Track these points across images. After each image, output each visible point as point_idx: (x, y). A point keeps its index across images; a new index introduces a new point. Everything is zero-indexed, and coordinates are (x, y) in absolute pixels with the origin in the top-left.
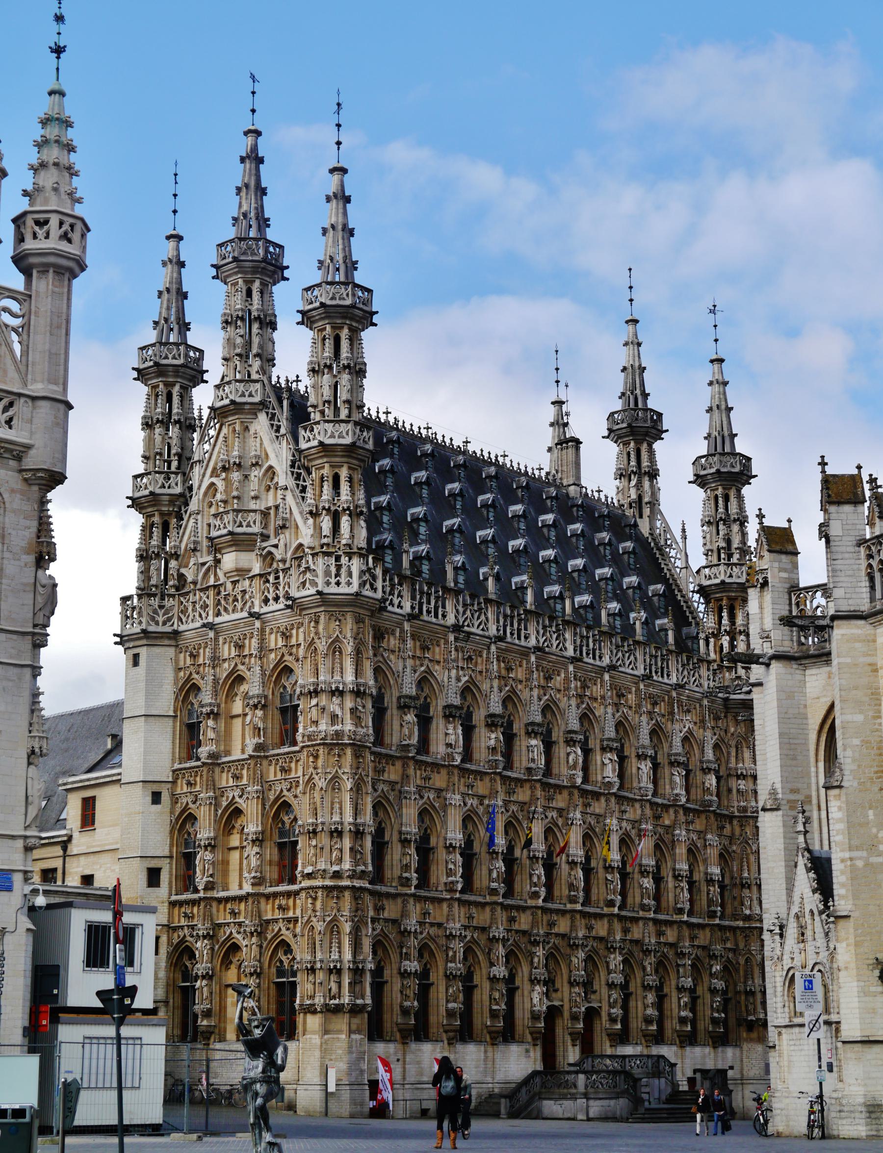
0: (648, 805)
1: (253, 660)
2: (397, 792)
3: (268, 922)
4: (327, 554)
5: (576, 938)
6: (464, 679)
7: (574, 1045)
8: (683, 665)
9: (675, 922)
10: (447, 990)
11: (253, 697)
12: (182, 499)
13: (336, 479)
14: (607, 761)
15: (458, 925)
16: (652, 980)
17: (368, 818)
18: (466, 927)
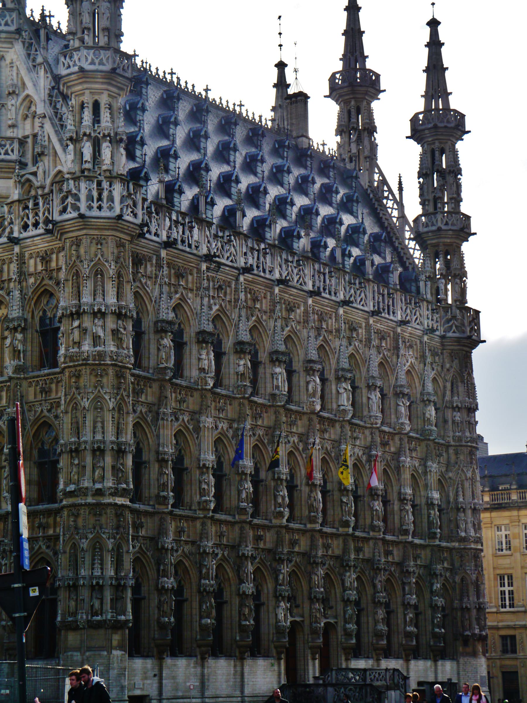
0: (377, 433)
1: (12, 285)
4: (89, 179)
5: (316, 556)
6: (215, 308)
7: (314, 659)
9: (401, 542)
11: (13, 320)
13: (96, 106)
14: (342, 391)
15: (210, 544)
16: (382, 596)
17: (129, 437)
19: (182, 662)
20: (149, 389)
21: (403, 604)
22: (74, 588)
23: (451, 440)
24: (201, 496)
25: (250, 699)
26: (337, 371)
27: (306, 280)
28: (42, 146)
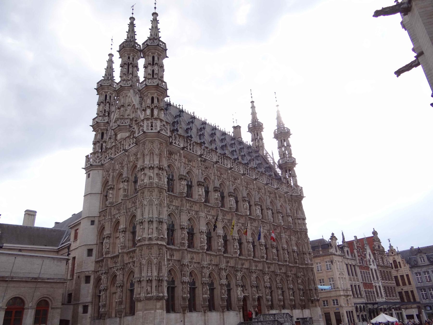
3: (127, 264)
5: (252, 269)
10: (203, 289)
15: (206, 263)
17: (164, 216)
18: (209, 264)
19: (194, 315)
20: (176, 201)
22: (140, 281)
23: (298, 229)
24: (201, 244)
26: (255, 202)
28: (136, 118)
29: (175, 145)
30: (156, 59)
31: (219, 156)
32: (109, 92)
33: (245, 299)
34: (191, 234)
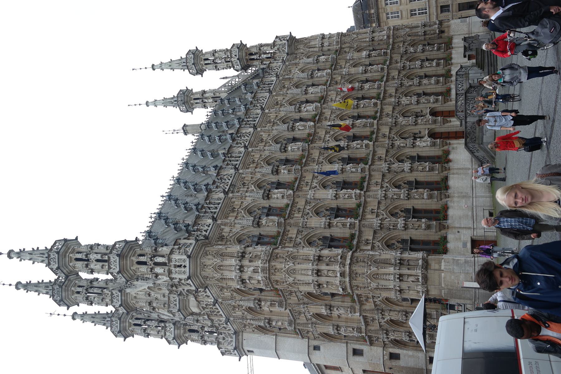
2: (303, 229)
3: (376, 305)
5: (392, 123)
6: (253, 188)
7: (450, 121)
8: (269, 75)
9: (388, 71)
10: (416, 199)
12: (177, 324)
16: (416, 81)
18: (382, 187)
20: (290, 232)
21: (421, 68)
24: (352, 198)
25: (473, 163)
27: (248, 132)
28: (168, 286)
29: (208, 231)
30: (79, 256)
31: (228, 164)
32: (130, 321)
33: (433, 135)
34: (338, 212)
